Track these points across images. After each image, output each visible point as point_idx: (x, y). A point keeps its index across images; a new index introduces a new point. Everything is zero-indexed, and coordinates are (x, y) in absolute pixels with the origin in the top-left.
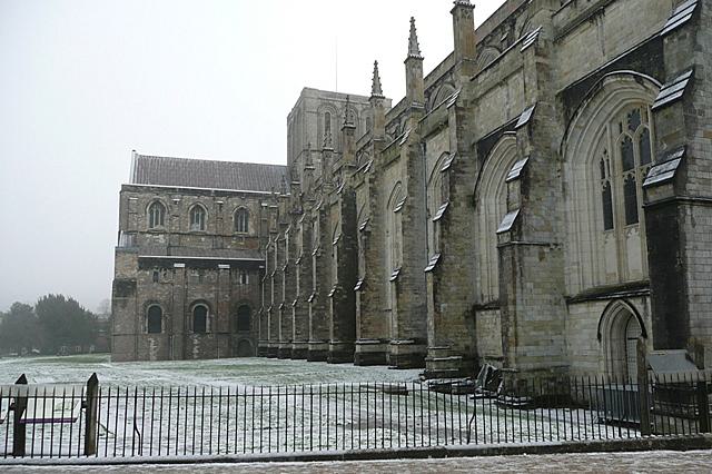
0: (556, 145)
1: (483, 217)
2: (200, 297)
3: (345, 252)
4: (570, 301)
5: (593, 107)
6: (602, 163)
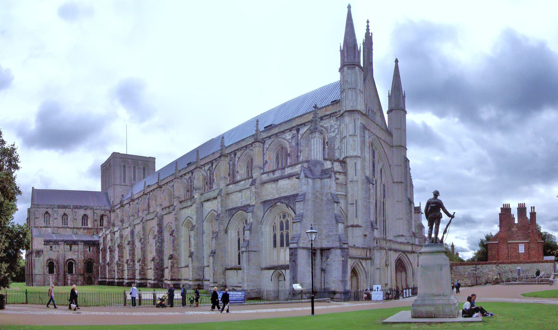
0: (260, 219)
1: (229, 237)
3: (159, 242)
4: (262, 269)
5: (273, 210)
6: (274, 227)
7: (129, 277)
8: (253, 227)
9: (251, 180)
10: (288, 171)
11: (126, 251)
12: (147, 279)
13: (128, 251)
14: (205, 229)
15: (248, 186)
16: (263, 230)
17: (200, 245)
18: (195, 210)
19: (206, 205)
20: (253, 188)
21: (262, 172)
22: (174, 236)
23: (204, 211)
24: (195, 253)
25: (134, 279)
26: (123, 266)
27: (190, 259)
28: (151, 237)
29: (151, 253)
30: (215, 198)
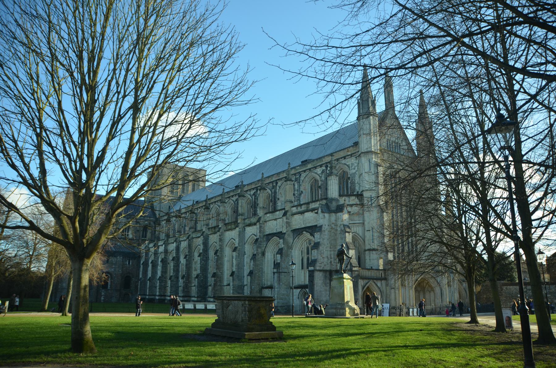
3: (203, 260)
8: (283, 251)
9: (283, 211)
10: (312, 206)
11: (170, 267)
13: (172, 267)
14: (246, 251)
15: (281, 216)
16: (293, 254)
17: (240, 266)
20: (284, 218)
21: (292, 205)
22: (218, 256)
23: (246, 234)
24: (236, 273)
26: (166, 282)
27: (231, 278)
28: (196, 254)
29: (196, 270)
30: (255, 224)
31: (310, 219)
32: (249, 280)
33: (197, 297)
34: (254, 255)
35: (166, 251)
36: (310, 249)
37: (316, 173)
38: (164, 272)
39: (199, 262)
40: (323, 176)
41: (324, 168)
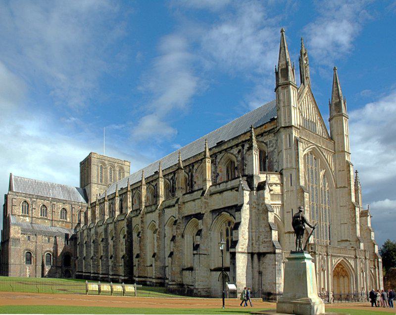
2: (48, 249)
4: (211, 270)
7: (104, 272)
9: (201, 191)
12: (119, 276)
13: (102, 248)
18: (158, 215)
19: (166, 210)
20: (203, 198)
25: (108, 274)
26: (98, 262)
27: (153, 259)
30: (174, 206)
31: (228, 199)
32: (170, 262)
33: (124, 276)
34: (174, 237)
35: (96, 233)
36: (229, 231)
37: (232, 154)
38: (96, 252)
39: (124, 244)
40: (239, 156)
41: (240, 147)
